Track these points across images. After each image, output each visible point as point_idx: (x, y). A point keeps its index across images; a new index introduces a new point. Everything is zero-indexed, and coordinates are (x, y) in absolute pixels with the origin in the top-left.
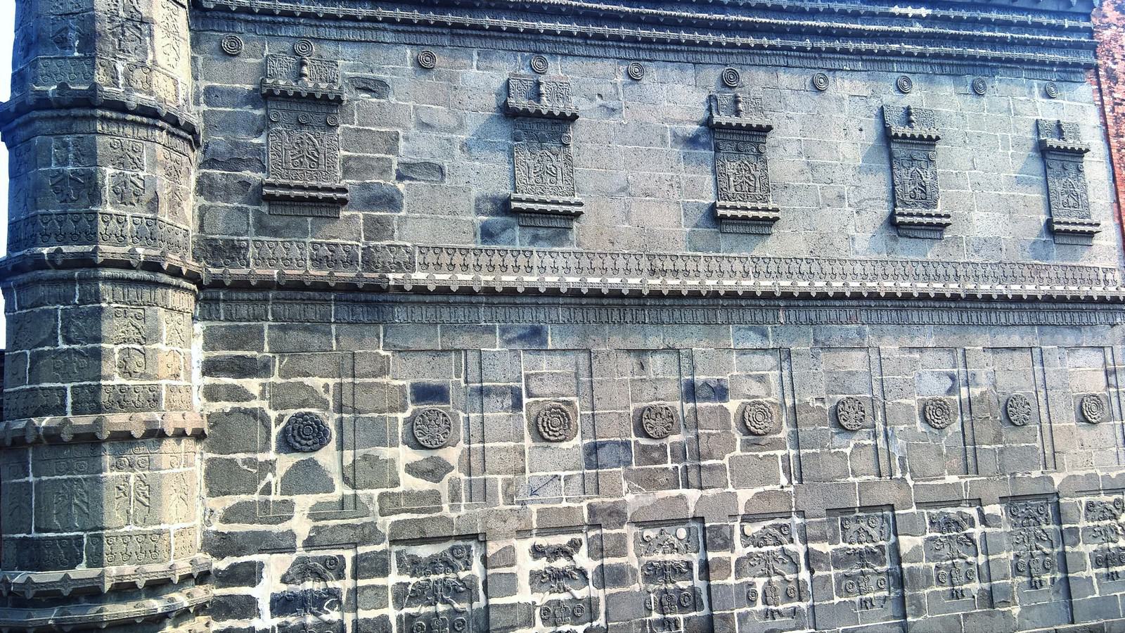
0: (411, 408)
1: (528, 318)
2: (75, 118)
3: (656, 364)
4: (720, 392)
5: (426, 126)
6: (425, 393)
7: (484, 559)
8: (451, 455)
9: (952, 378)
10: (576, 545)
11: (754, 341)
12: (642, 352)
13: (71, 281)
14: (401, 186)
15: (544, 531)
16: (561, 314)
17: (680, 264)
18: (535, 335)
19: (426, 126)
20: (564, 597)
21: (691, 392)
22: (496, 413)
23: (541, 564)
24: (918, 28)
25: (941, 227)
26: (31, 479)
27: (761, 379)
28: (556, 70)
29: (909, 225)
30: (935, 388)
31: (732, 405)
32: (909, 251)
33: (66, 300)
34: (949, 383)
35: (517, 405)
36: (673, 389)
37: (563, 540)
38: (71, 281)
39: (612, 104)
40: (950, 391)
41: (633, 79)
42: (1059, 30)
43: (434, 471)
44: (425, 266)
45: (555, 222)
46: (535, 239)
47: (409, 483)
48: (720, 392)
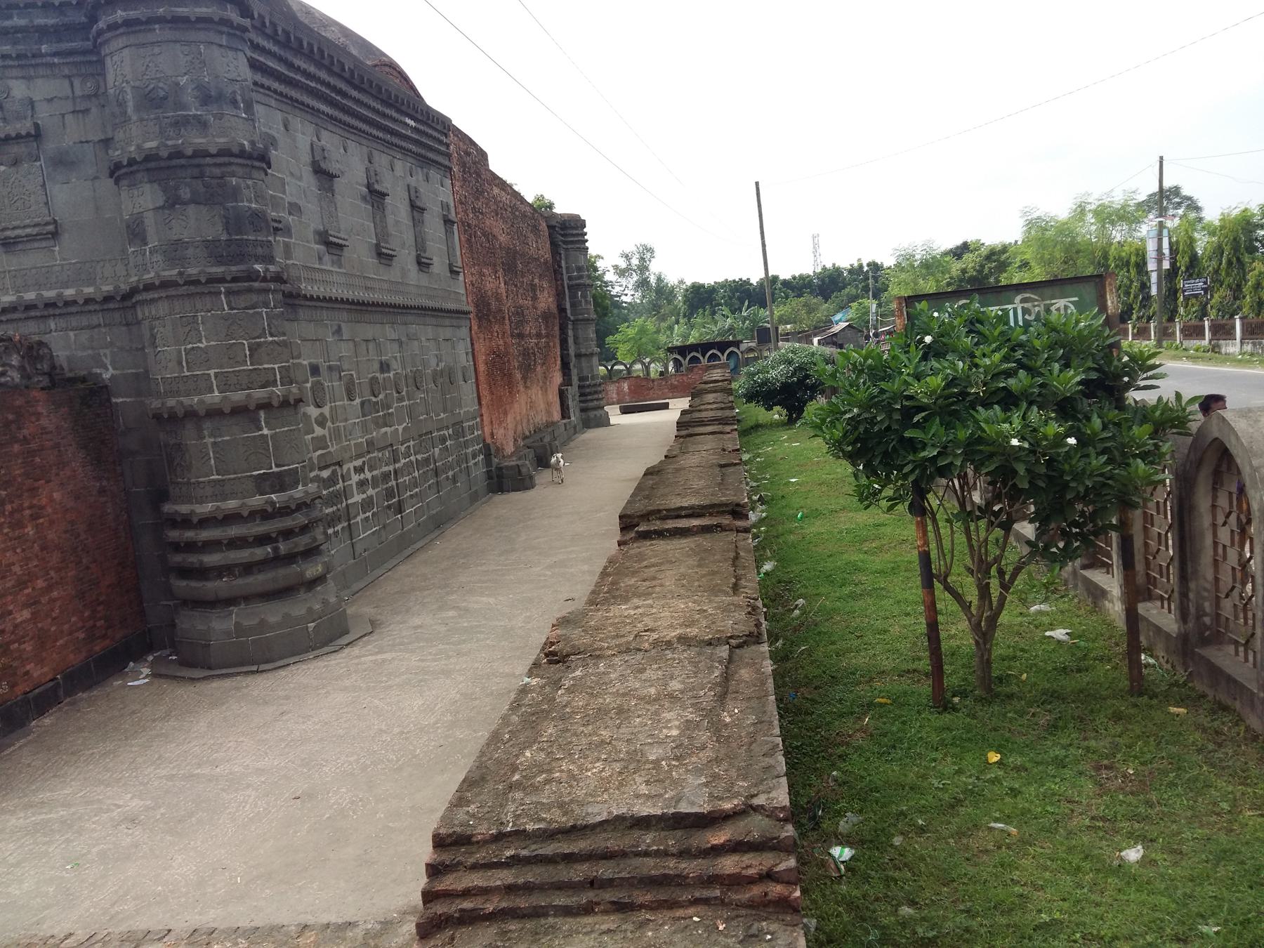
2: (253, 167)
7: (342, 476)
8: (326, 410)
13: (267, 291)
15: (359, 456)
20: (364, 496)
26: (265, 431)
31: (391, 375)
33: (266, 305)
36: (376, 366)
38: (267, 291)
43: (321, 422)
47: (319, 431)
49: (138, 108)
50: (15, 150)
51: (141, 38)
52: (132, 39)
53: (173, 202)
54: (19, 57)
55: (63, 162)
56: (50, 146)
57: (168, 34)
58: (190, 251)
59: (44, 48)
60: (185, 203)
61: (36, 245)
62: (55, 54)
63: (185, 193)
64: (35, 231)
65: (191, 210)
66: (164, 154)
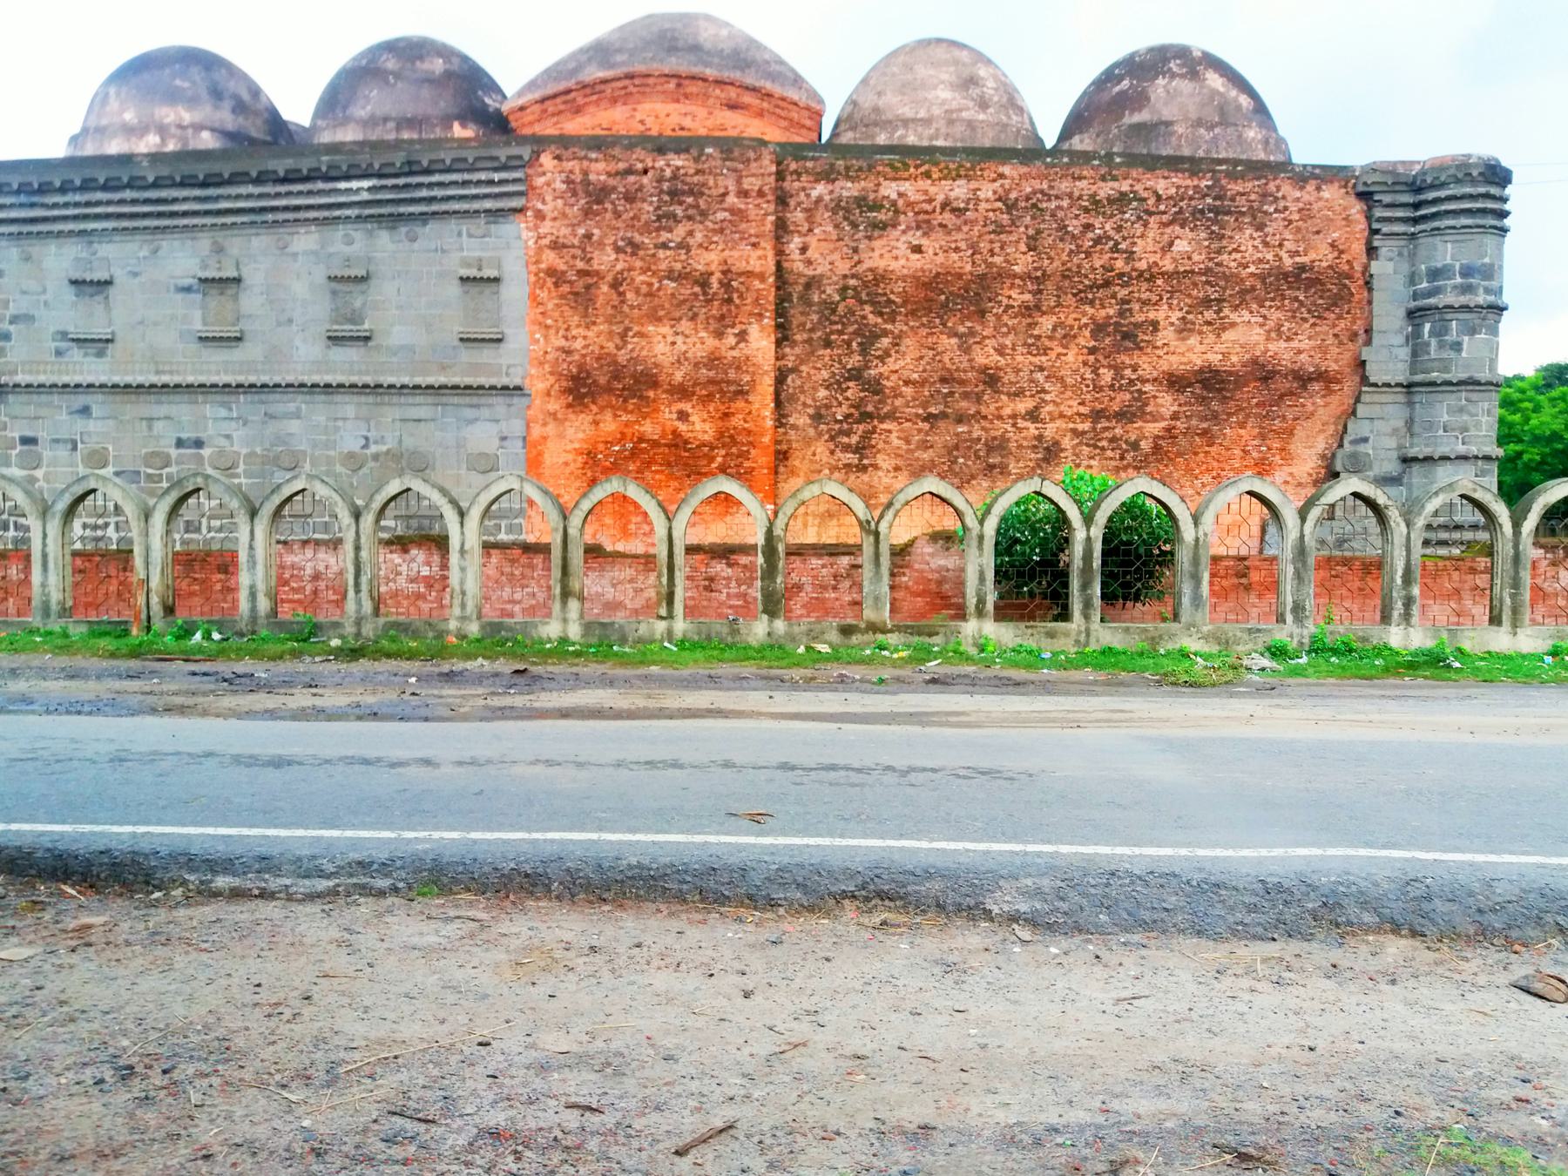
0: (19, 448)
1: (81, 400)
3: (159, 426)
4: (199, 444)
5: (24, 293)
6: (28, 441)
8: (39, 473)
9: (367, 439)
10: (107, 525)
11: (223, 413)
12: (151, 419)
14: (12, 328)
16: (100, 397)
17: (175, 367)
18: (85, 411)
19: (24, 293)
21: (180, 443)
22: (63, 452)
23: (88, 532)
24: (365, 196)
25: (367, 339)
27: (228, 437)
28: (106, 249)
29: (349, 335)
30: (354, 445)
31: (206, 452)
32: (341, 354)
34: (363, 442)
35: (75, 448)
37: (100, 522)
39: (136, 270)
40: (365, 446)
41: (156, 251)
42: (491, 182)
44: (23, 372)
45: (100, 345)
46: (86, 355)
48: (199, 444)
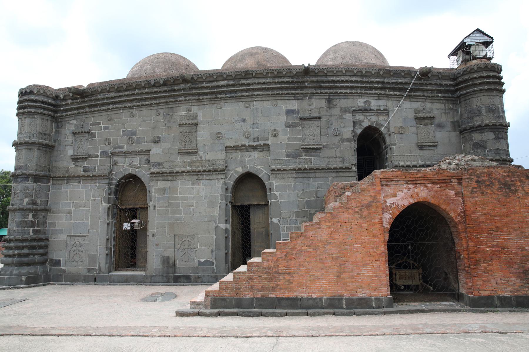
49: (486, 112)
50: (427, 121)
51: (489, 94)
52: (486, 94)
53: (497, 138)
54: (432, 96)
55: (440, 126)
56: (436, 121)
57: (497, 94)
58: (501, 152)
59: (440, 95)
60: (500, 138)
61: (430, 148)
62: (443, 97)
63: (500, 136)
64: (432, 144)
65: (502, 140)
66: (498, 124)
